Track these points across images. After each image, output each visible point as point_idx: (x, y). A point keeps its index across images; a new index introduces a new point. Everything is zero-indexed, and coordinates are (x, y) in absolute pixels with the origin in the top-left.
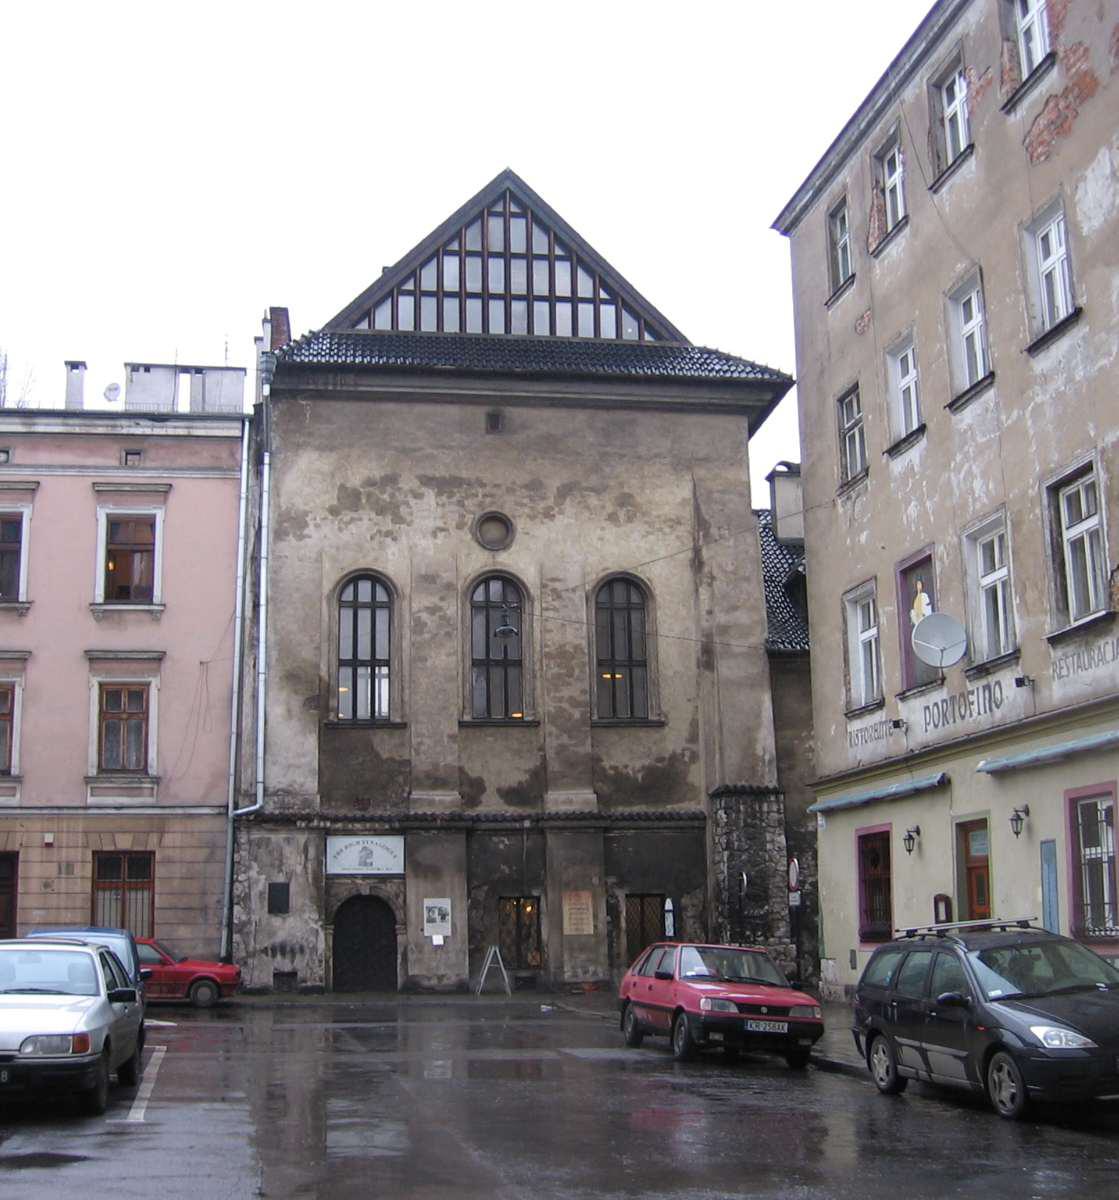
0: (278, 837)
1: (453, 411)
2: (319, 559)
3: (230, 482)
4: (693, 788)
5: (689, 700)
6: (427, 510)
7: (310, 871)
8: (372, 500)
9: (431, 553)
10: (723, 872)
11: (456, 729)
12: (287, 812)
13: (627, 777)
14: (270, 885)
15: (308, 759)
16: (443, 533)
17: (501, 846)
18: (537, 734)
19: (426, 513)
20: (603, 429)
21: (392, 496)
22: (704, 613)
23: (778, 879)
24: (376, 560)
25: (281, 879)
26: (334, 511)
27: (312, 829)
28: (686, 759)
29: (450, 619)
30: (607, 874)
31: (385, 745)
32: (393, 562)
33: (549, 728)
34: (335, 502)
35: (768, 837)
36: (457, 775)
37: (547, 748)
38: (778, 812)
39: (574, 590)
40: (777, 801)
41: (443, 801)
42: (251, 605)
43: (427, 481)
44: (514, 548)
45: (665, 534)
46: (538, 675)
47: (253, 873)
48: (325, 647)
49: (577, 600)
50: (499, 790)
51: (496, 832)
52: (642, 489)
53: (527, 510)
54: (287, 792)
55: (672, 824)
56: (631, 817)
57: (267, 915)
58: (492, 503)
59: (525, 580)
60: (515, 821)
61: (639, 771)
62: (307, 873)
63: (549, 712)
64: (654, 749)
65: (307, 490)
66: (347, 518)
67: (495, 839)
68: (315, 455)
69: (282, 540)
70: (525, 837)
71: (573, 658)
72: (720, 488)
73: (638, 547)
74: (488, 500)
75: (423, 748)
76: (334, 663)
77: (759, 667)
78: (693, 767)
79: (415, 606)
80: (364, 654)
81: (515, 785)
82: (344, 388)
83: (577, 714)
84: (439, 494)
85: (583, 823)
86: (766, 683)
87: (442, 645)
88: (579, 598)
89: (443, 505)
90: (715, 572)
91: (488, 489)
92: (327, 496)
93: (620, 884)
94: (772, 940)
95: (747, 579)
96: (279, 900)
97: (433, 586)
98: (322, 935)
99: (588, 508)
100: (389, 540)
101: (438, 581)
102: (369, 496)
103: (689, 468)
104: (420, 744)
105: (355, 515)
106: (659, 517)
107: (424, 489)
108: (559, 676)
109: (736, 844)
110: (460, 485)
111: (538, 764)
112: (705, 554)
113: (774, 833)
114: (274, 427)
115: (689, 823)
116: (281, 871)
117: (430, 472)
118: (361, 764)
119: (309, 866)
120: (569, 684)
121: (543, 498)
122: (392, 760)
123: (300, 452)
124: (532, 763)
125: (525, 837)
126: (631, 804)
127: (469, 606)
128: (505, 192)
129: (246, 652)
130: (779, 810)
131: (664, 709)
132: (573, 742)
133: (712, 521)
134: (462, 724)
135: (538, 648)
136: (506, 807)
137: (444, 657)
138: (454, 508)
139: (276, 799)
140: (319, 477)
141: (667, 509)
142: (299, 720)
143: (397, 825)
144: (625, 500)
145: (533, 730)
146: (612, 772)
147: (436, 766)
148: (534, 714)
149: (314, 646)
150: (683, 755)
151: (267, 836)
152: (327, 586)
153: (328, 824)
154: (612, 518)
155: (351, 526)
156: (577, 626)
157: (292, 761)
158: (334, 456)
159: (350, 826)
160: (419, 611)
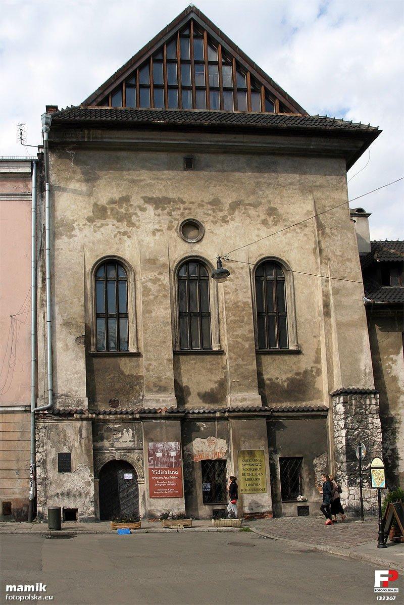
0: (64, 425)
1: (163, 156)
5: (315, 337)
6: (149, 218)
7: (83, 445)
8: (116, 212)
9: (152, 245)
10: (341, 443)
13: (278, 385)
16: (159, 233)
19: (148, 221)
21: (127, 210)
22: (324, 281)
23: (375, 447)
24: (118, 250)
25: (65, 450)
26: (90, 220)
28: (314, 373)
32: (128, 251)
34: (91, 214)
35: (370, 420)
41: (166, 401)
43: (148, 200)
44: (204, 241)
47: (47, 447)
49: (244, 276)
52: (283, 204)
53: (211, 218)
54: (67, 396)
57: (57, 473)
61: (285, 381)
62: (81, 447)
64: (294, 367)
65: (73, 206)
66: (99, 224)
71: (243, 310)
73: (281, 241)
74: (187, 212)
75: (151, 368)
78: (318, 378)
81: (208, 390)
83: (247, 345)
84: (156, 208)
89: (159, 215)
90: (330, 256)
91: (186, 205)
92: (86, 211)
95: (349, 260)
96: (64, 463)
97: (154, 266)
98: (93, 484)
99: (249, 217)
100: (125, 237)
101: (157, 262)
102: (112, 210)
103: (311, 192)
104: (150, 364)
105: (104, 222)
107: (146, 205)
108: (234, 321)
110: (169, 203)
112: (323, 245)
113: (373, 418)
116: (65, 445)
117: (150, 195)
119: (83, 441)
120: (242, 327)
121: (221, 210)
122: (132, 376)
123: (68, 184)
124: (218, 377)
126: (281, 402)
128: (189, 22)
129: (39, 307)
136: (204, 405)
137: (162, 310)
138: (166, 217)
141: (298, 217)
142: (73, 350)
143: (138, 416)
144: (272, 211)
145: (219, 356)
146: (268, 382)
147: (159, 378)
152: (89, 267)
153: (94, 416)
154: (264, 222)
155: (102, 229)
156: (245, 290)
157: (69, 377)
159: (107, 417)
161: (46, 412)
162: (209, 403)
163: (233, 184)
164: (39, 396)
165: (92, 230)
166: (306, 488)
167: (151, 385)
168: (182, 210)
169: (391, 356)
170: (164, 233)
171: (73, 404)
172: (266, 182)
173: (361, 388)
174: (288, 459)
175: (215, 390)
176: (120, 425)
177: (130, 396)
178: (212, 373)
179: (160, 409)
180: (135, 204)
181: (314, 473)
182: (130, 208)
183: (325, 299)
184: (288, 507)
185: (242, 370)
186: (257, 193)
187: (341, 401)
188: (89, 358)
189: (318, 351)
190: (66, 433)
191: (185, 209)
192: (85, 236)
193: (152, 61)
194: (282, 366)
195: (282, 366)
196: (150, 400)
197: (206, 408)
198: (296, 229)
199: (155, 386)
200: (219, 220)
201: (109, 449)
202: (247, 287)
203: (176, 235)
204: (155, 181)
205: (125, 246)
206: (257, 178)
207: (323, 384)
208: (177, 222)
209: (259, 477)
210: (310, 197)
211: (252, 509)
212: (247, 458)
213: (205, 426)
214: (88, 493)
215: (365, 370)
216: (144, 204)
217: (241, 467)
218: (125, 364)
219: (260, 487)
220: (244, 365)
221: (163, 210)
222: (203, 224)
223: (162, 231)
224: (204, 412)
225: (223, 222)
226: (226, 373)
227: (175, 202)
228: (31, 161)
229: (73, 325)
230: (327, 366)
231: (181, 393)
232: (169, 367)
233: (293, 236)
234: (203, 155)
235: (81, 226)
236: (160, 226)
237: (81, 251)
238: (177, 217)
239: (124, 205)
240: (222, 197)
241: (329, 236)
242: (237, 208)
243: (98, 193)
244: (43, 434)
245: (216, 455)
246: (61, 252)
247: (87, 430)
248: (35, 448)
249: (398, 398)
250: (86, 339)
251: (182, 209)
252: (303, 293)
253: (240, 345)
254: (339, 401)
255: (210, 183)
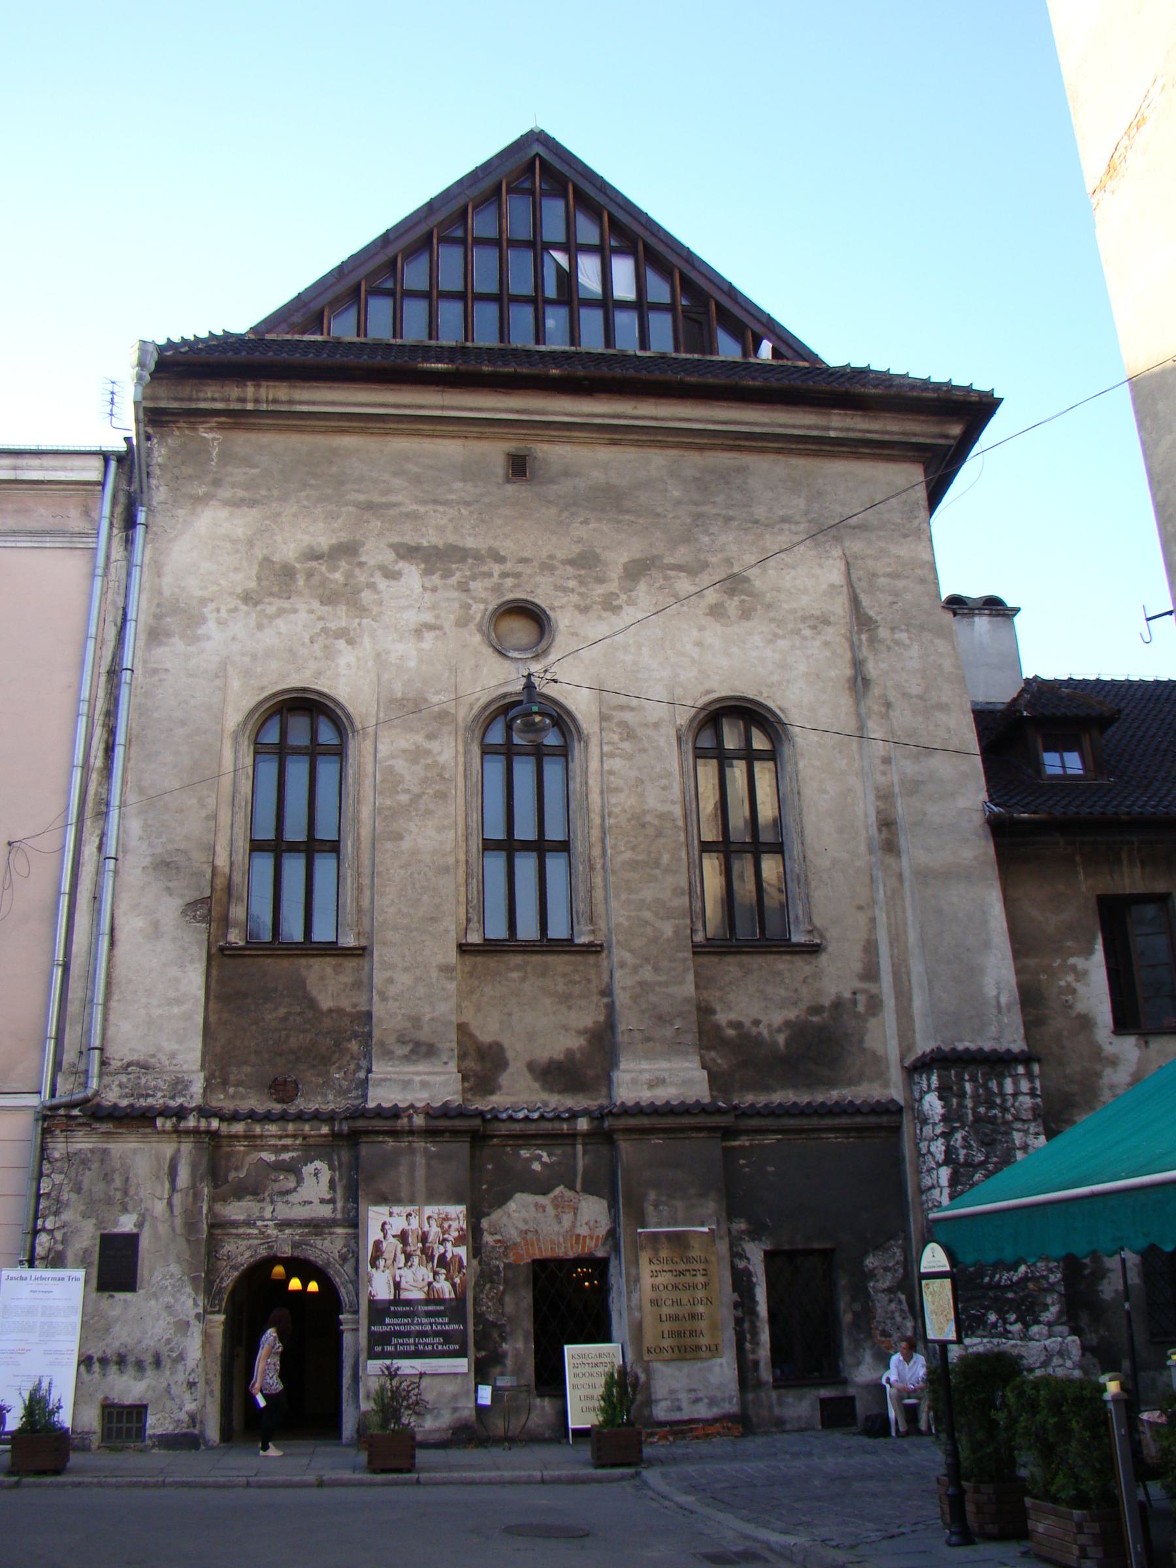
1: (451, 449)
2: (221, 672)
3: (78, 552)
4: (878, 1061)
5: (860, 908)
6: (407, 596)
7: (177, 1210)
9: (412, 664)
11: (452, 956)
12: (143, 1103)
13: (758, 1041)
14: (103, 1236)
15: (185, 1008)
17: (536, 1166)
18: (597, 965)
19: (404, 602)
20: (695, 479)
21: (349, 575)
22: (878, 761)
24: (318, 674)
26: (248, 598)
27: (187, 1132)
28: (861, 1008)
29: (443, 768)
30: (732, 1212)
31: (328, 986)
32: (347, 680)
33: (619, 954)
34: (253, 585)
36: (454, 1036)
37: (617, 990)
38: (1032, 1093)
39: (656, 725)
40: (1030, 1076)
41: (432, 1084)
42: (102, 746)
43: (408, 552)
45: (805, 638)
46: (598, 866)
48: (224, 817)
50: (531, 1067)
51: (526, 1139)
53: (575, 598)
54: (145, 1067)
55: (844, 1121)
56: (771, 1112)
58: (515, 586)
59: (572, 707)
60: (558, 1118)
61: (779, 1030)
63: (618, 925)
64: (804, 991)
67: (522, 1152)
68: (224, 513)
69: (160, 644)
70: (580, 1148)
71: (659, 835)
72: (889, 570)
74: (509, 582)
76: (242, 845)
77: (978, 849)
78: (872, 1023)
79: (384, 750)
80: (295, 831)
81: (559, 1056)
82: (272, 407)
83: (668, 930)
84: (427, 572)
85: (686, 1121)
86: (993, 873)
87: (429, 812)
88: (666, 740)
89: (434, 590)
90: (893, 696)
91: (508, 566)
92: (239, 577)
93: (755, 1234)
94: (1035, 1329)
95: (942, 707)
98: (196, 1330)
100: (341, 644)
102: (310, 575)
103: (838, 539)
105: (286, 605)
106: (795, 611)
107: (402, 565)
109: (962, 1152)
110: (463, 559)
111: (602, 1018)
112: (872, 669)
114: (158, 472)
115: (873, 1120)
117: (410, 539)
118: (284, 1019)
119: (177, 1199)
121: (601, 581)
122: (340, 1011)
123: (199, 509)
124: (588, 1017)
125: (580, 1148)
126: (768, 1089)
127: (476, 750)
130: (1033, 1089)
131: (818, 922)
132: (663, 978)
133: (879, 618)
134: (464, 949)
135: (597, 821)
136: (545, 1096)
138: (456, 594)
139: (124, 1078)
140: (228, 545)
141: (805, 600)
144: (734, 583)
145: (591, 959)
146: (731, 1032)
147: (416, 1021)
148: (593, 932)
149: (204, 814)
150: (855, 1003)
151: (105, 1146)
152: (234, 718)
154: (716, 611)
155: (280, 623)
158: (254, 513)
159: (258, 1129)
160: (392, 757)
161: (76, 1112)
162: (560, 1092)
163: (632, 518)
164: (65, 1065)
165: (252, 622)
166: (846, 1343)
167: (391, 1040)
168: (496, 579)
169: (1072, 961)
170: (445, 634)
171: (160, 1090)
172: (719, 515)
173: (987, 1046)
174: (791, 1255)
175: (578, 1056)
176: (294, 1154)
177: (333, 1069)
178: (570, 1008)
179: (412, 1106)
180: (372, 563)
181: (868, 1296)
182: (357, 571)
183: (882, 806)
184: (790, 1400)
185: (652, 998)
186: (696, 540)
187: (933, 1086)
188: (221, 957)
189: (871, 948)
190: (131, 1175)
191: (504, 575)
192: (234, 639)
193: (435, 241)
194: (770, 989)
195: (770, 989)
196: (384, 1080)
197: (552, 1105)
198: (800, 630)
199: (402, 1041)
200: (595, 603)
201: (259, 1223)
202: (668, 774)
203: (477, 638)
204: (430, 507)
205: (337, 665)
206: (696, 504)
207: (884, 1038)
208: (482, 607)
209: (701, 1309)
210: (837, 552)
211: (679, 1409)
212: (664, 1253)
213: (546, 1158)
214: (181, 1358)
215: (997, 997)
216: (396, 562)
217: (647, 1281)
218: (322, 978)
219: (704, 1341)
220: (660, 984)
221: (444, 577)
222: (549, 612)
223: (440, 628)
224: (542, 1117)
225: (605, 610)
226: (611, 1008)
227: (477, 556)
228: (106, 456)
229: (177, 868)
230: (895, 985)
231: (483, 1063)
232: (444, 989)
233: (793, 647)
234: (557, 448)
235: (224, 614)
236: (437, 617)
237: (217, 677)
238: (483, 595)
239: (343, 563)
240: (604, 548)
241: (889, 648)
242: (644, 576)
243: (274, 534)
244: (62, 1176)
245: (577, 1242)
246: (164, 676)
247: (194, 1167)
248: (36, 1218)
249: (1098, 1075)
250: (210, 908)
251: (496, 575)
252: (823, 791)
253: (649, 930)
254: (929, 1085)
255: (573, 514)
